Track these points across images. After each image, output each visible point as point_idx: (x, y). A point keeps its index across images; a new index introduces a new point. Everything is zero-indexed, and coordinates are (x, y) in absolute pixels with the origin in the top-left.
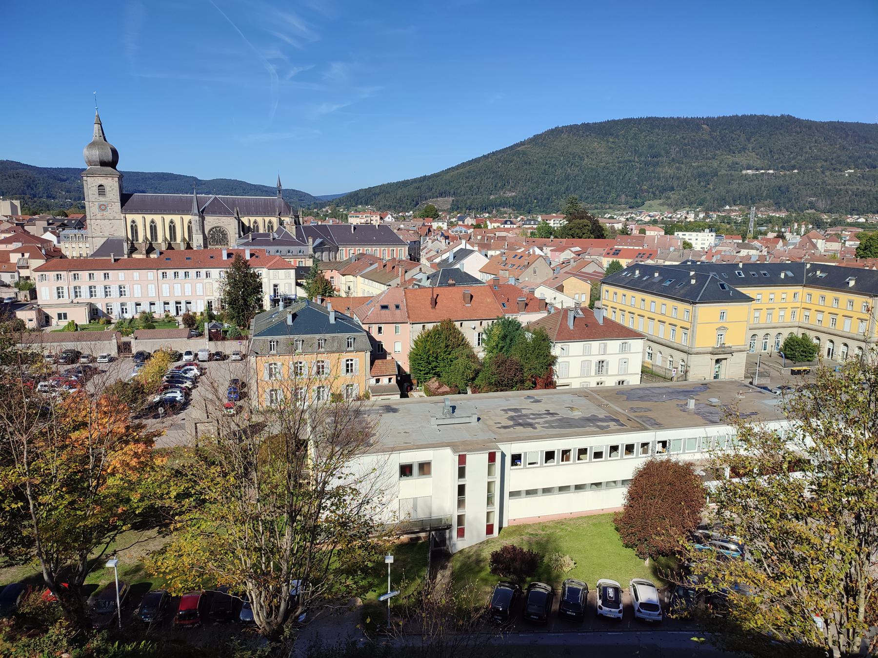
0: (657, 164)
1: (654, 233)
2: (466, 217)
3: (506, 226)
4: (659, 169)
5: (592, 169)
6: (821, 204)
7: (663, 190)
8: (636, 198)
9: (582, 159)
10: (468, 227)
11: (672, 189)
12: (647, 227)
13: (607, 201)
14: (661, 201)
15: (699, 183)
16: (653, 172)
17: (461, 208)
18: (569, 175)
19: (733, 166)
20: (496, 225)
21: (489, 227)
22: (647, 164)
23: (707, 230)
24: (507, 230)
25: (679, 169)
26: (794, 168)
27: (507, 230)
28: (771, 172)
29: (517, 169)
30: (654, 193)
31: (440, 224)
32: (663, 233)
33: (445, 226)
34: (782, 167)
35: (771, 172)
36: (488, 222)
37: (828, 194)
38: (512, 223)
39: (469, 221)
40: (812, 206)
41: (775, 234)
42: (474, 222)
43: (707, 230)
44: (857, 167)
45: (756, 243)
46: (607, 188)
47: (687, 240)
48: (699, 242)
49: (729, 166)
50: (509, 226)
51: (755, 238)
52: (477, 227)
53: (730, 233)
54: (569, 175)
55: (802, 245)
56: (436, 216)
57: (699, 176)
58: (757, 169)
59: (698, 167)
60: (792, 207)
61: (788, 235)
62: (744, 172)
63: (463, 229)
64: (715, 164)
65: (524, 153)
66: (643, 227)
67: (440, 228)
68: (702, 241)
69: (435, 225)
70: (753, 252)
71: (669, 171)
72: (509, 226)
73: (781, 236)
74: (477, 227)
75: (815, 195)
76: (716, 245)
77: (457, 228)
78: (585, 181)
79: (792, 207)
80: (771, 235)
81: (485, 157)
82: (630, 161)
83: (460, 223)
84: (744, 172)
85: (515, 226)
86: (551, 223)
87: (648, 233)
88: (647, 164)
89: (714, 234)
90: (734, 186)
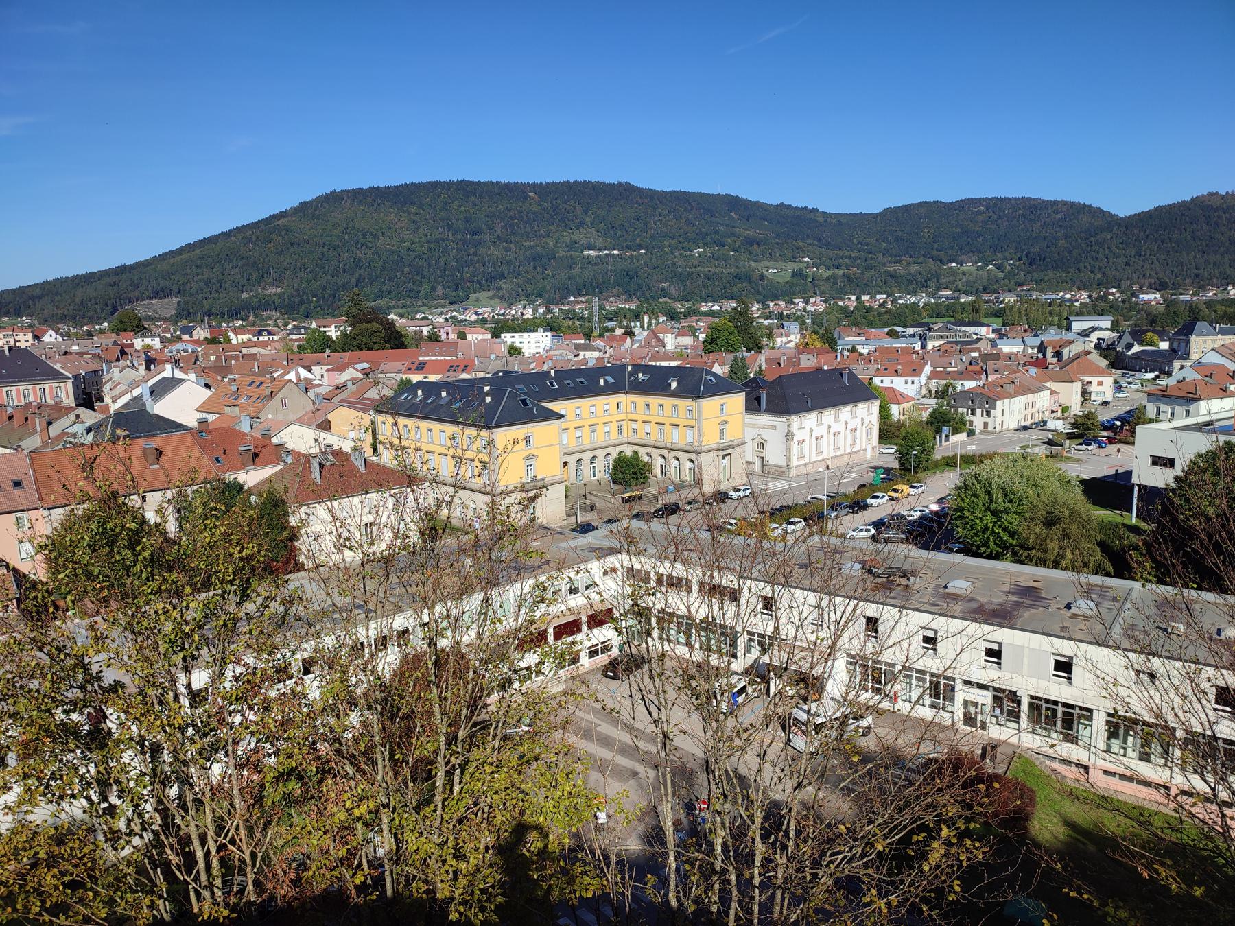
0: (478, 244)
1: (476, 337)
2: (194, 328)
3: (261, 338)
4: (482, 251)
5: (393, 252)
6: (674, 291)
7: (492, 279)
8: (456, 290)
9: (376, 238)
10: (198, 342)
11: (502, 276)
12: (467, 330)
13: (413, 299)
14: (490, 293)
15: (535, 268)
16: (475, 254)
17: (187, 315)
18: (360, 261)
19: (573, 246)
20: (246, 337)
21: (234, 342)
22: (465, 243)
23: (540, 330)
24: (264, 345)
25: (507, 250)
26: (640, 247)
27: (264, 345)
28: (616, 252)
29: (280, 253)
30: (479, 282)
31: (148, 341)
32: (488, 336)
33: (157, 344)
34: (627, 247)
35: (616, 252)
36: (231, 334)
37: (680, 278)
38: (270, 333)
39: (201, 333)
40: (665, 293)
41: (623, 331)
42: (208, 336)
43: (540, 330)
44: (705, 245)
45: (599, 343)
46: (416, 277)
47: (517, 345)
48: (533, 345)
49: (567, 246)
50: (266, 338)
51: (601, 336)
52: (213, 341)
53: (572, 331)
54: (360, 261)
55: (648, 341)
56: (139, 328)
57: (534, 259)
58: (600, 250)
59: (531, 247)
60: (643, 295)
61: (637, 331)
62: (585, 253)
63: (190, 347)
64: (551, 243)
65: (287, 229)
66: (461, 329)
67: (147, 348)
68: (535, 344)
69: (139, 343)
70: (596, 354)
71: (495, 252)
72: (266, 338)
73: (629, 333)
74: (213, 341)
75: (666, 281)
76: (551, 348)
77: (179, 346)
78: (383, 268)
79: (643, 295)
80: (619, 332)
81: (225, 235)
82: (443, 240)
83: (186, 337)
84: (585, 253)
85: (275, 338)
86: (333, 332)
87: (469, 337)
88: (465, 243)
89: (549, 334)
90: (577, 271)
